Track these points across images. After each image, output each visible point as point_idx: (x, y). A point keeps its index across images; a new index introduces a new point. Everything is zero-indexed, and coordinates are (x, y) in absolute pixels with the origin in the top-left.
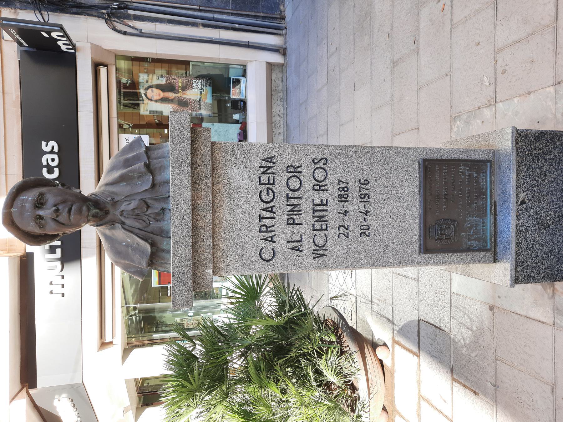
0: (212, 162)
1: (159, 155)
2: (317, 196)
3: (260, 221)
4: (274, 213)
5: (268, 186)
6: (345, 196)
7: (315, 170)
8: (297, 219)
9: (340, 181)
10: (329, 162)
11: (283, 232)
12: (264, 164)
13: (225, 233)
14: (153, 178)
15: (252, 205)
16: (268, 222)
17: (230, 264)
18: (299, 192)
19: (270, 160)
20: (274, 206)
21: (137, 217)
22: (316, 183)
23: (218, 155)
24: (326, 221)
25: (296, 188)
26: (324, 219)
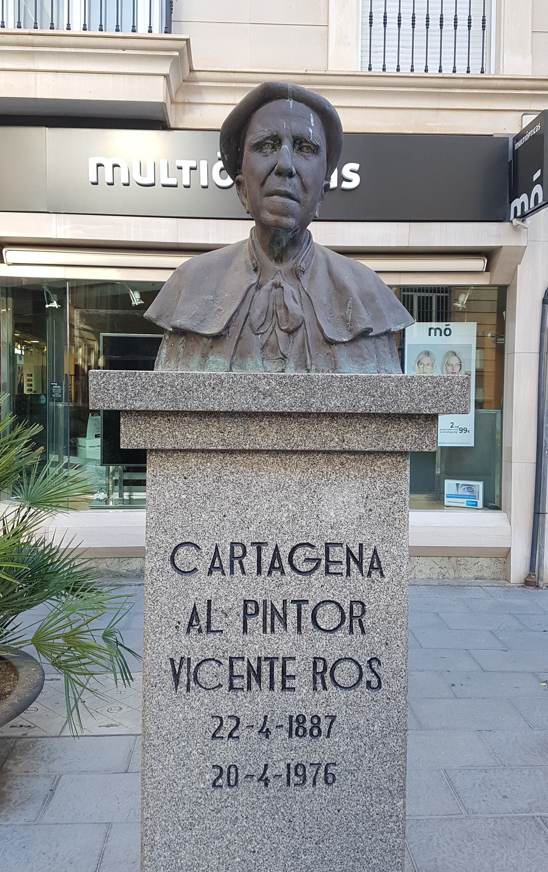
0: (370, 453)
1: (382, 354)
2: (302, 667)
3: (253, 544)
4: (270, 573)
5: (323, 562)
6: (301, 731)
7: (356, 663)
8: (255, 623)
9: (333, 718)
10: (373, 693)
11: (229, 592)
12: (368, 554)
13: (232, 473)
14: (344, 343)
15: (286, 528)
16: (250, 561)
17: (171, 483)
18: (311, 627)
19: (376, 565)
20: (283, 573)
21: (270, 314)
22: (330, 665)
23: (383, 464)
24: (249, 688)
25: (319, 621)
26: (254, 683)
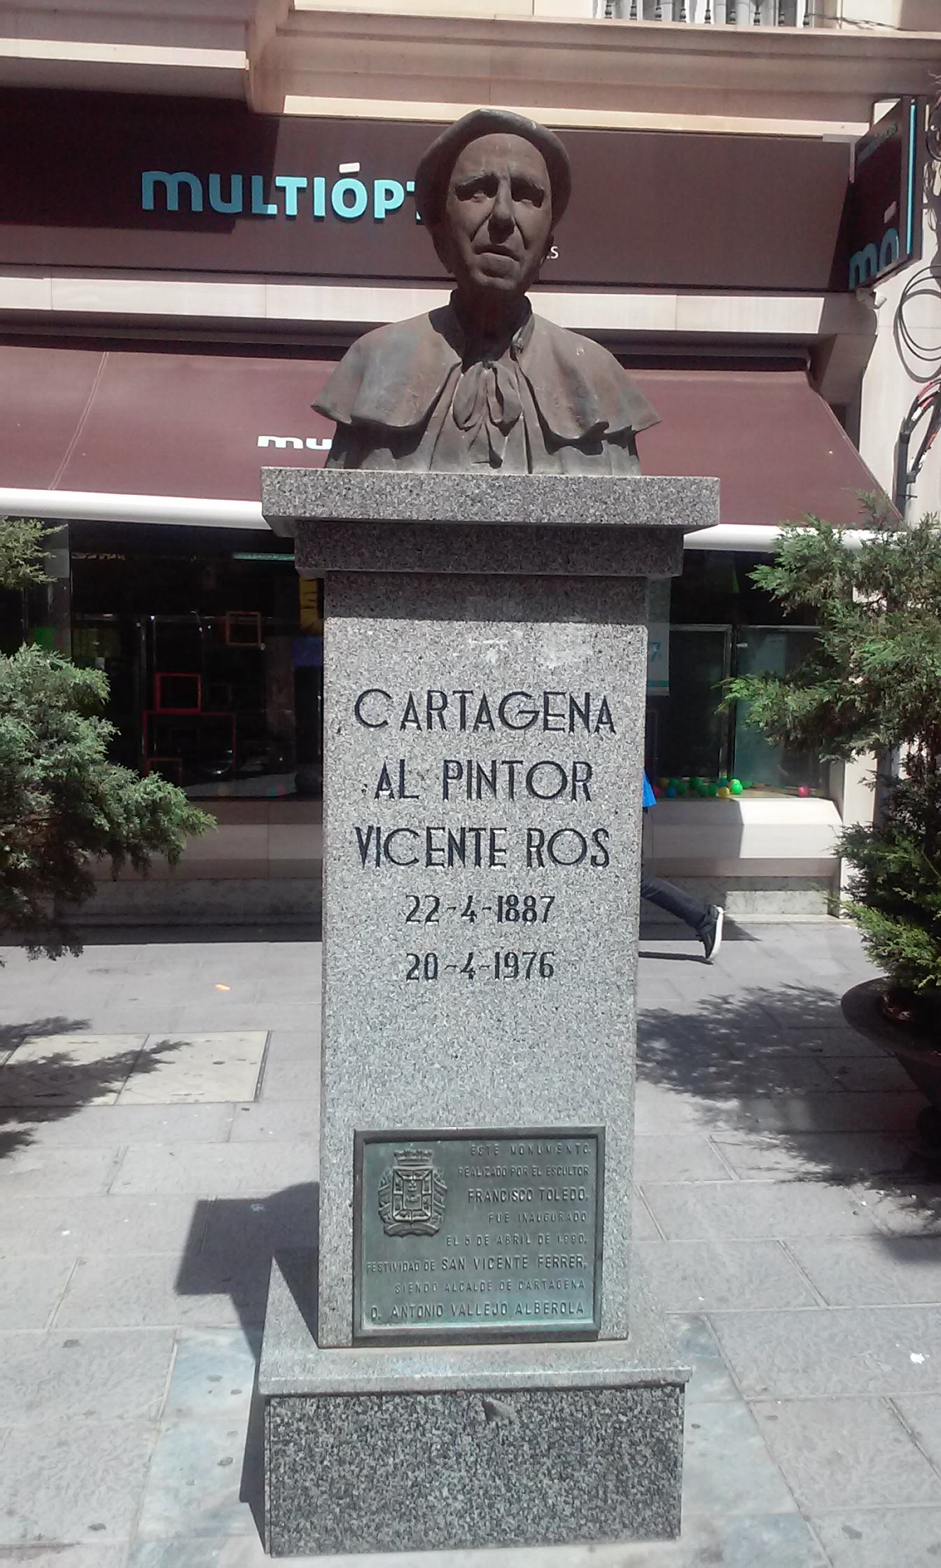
5: (541, 715)
11: (425, 751)
12: (596, 705)
20: (492, 728)
22: (548, 838)
24: (451, 863)
26: (456, 857)
